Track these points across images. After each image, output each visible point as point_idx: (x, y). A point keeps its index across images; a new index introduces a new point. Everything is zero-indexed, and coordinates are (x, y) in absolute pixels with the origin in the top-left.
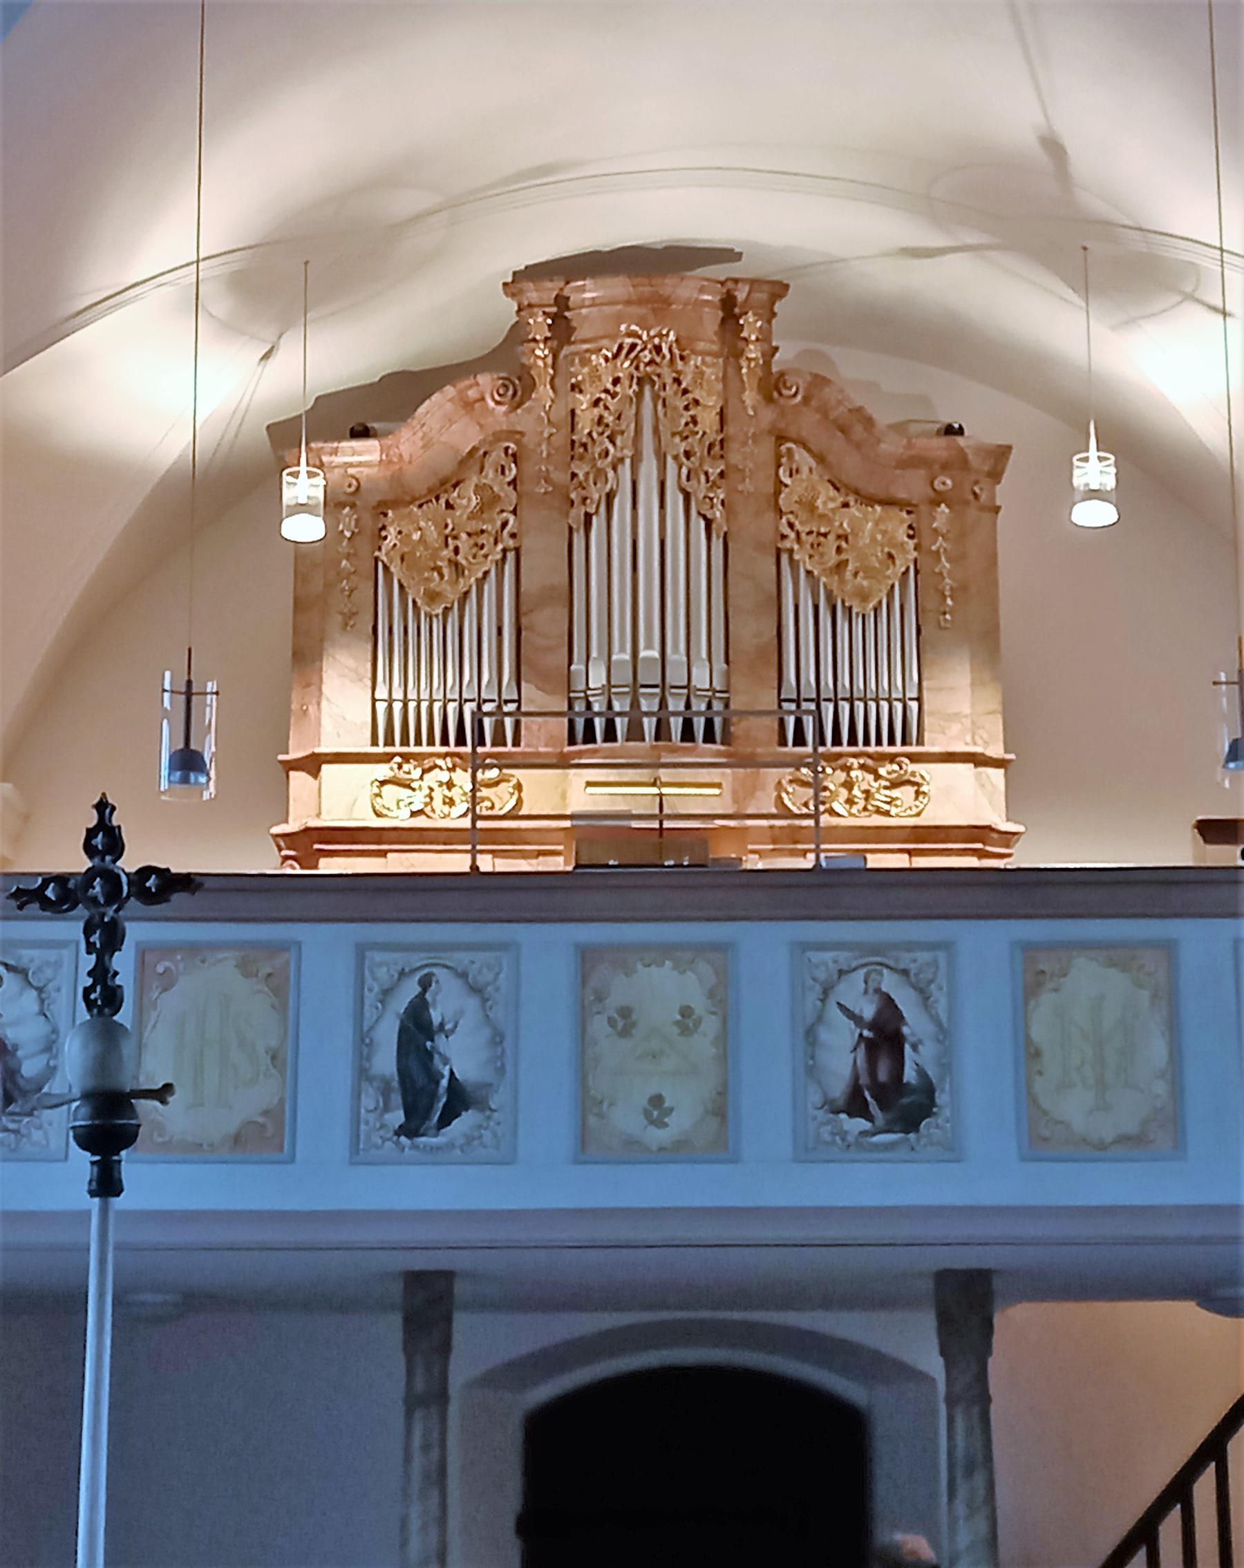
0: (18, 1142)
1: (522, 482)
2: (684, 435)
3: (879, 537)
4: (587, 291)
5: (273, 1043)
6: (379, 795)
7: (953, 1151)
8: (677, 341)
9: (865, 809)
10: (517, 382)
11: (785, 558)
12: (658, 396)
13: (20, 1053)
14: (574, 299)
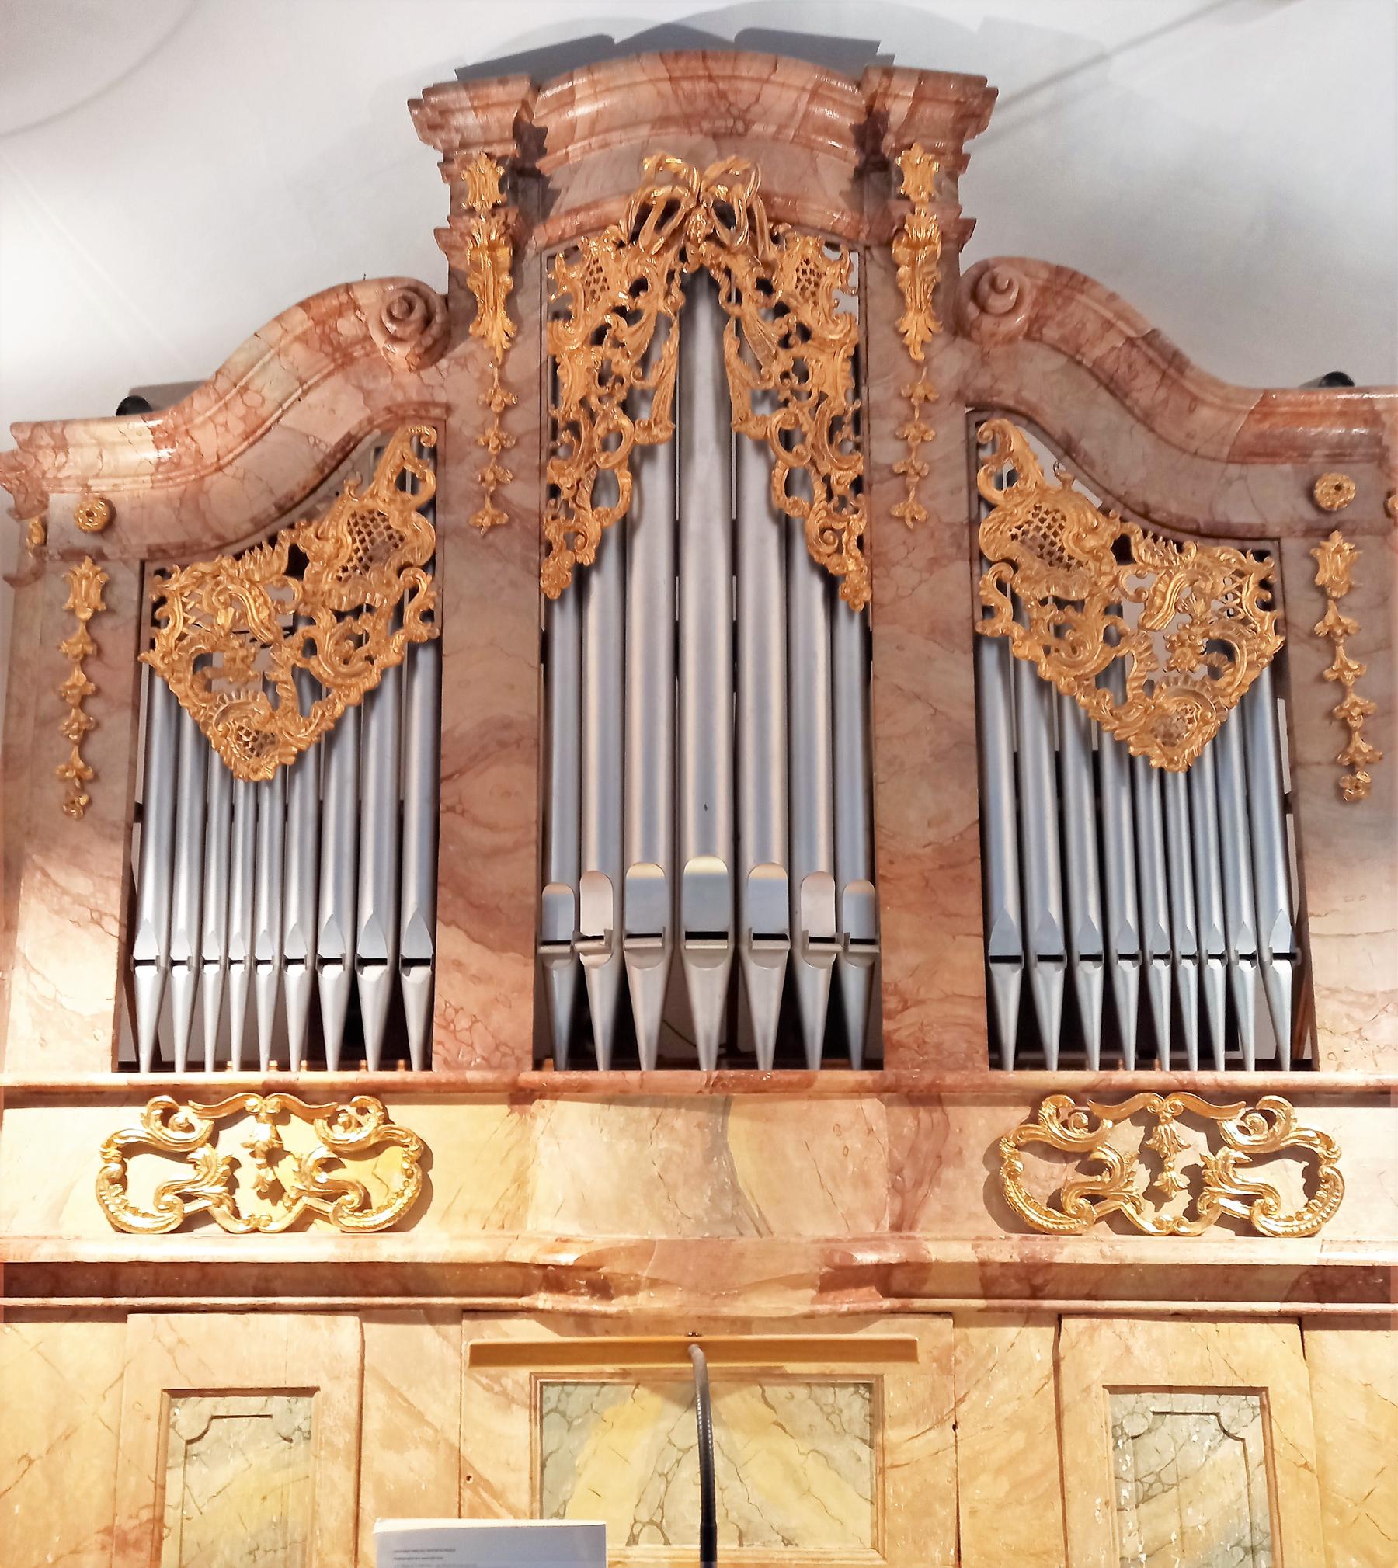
1: (446, 502)
2: (781, 398)
11: (990, 656)
12: (725, 317)
14: (552, 123)
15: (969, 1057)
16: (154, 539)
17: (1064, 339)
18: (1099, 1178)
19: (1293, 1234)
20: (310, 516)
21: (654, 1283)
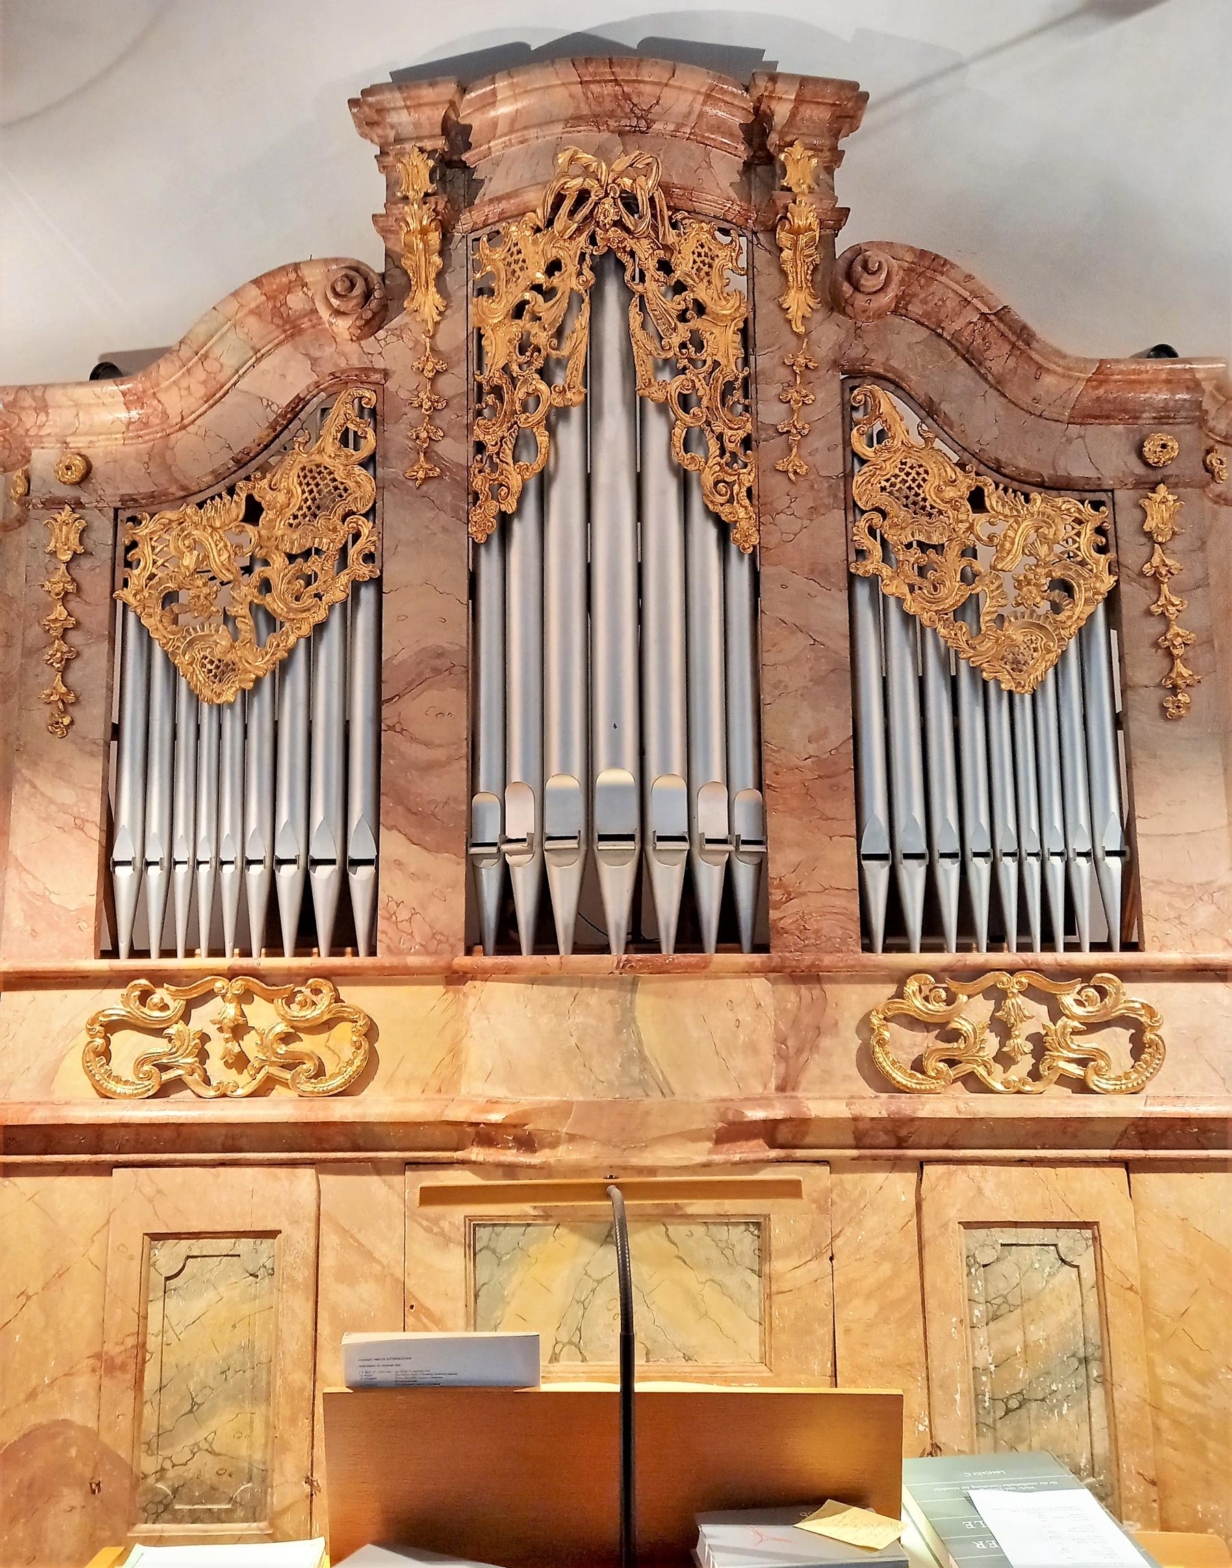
1: (385, 457)
2: (680, 366)
11: (862, 593)
14: (477, 121)
15: (844, 942)
16: (127, 490)
17: (926, 314)
18: (955, 1045)
19: (1121, 1092)
20: (264, 469)
21: (572, 1138)
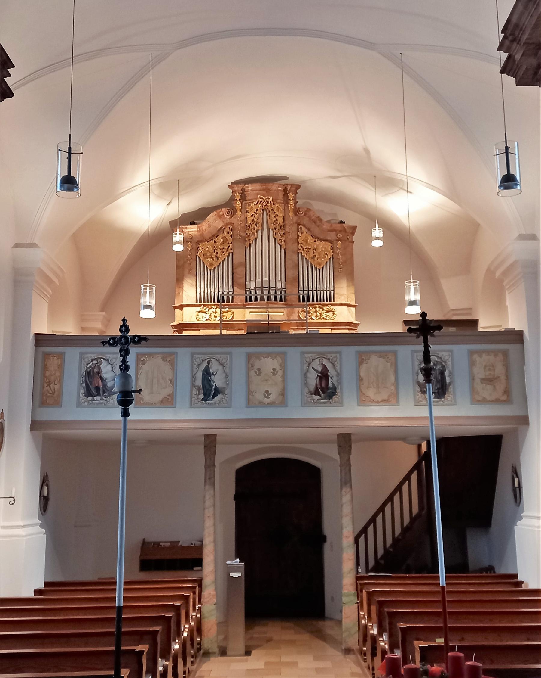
0: (107, 403)
3: (324, 249)
4: (250, 187)
5: (171, 378)
6: (198, 315)
7: (341, 404)
8: (272, 200)
9: (320, 318)
10: (232, 210)
11: (300, 255)
13: (107, 381)
16: (198, 240)
